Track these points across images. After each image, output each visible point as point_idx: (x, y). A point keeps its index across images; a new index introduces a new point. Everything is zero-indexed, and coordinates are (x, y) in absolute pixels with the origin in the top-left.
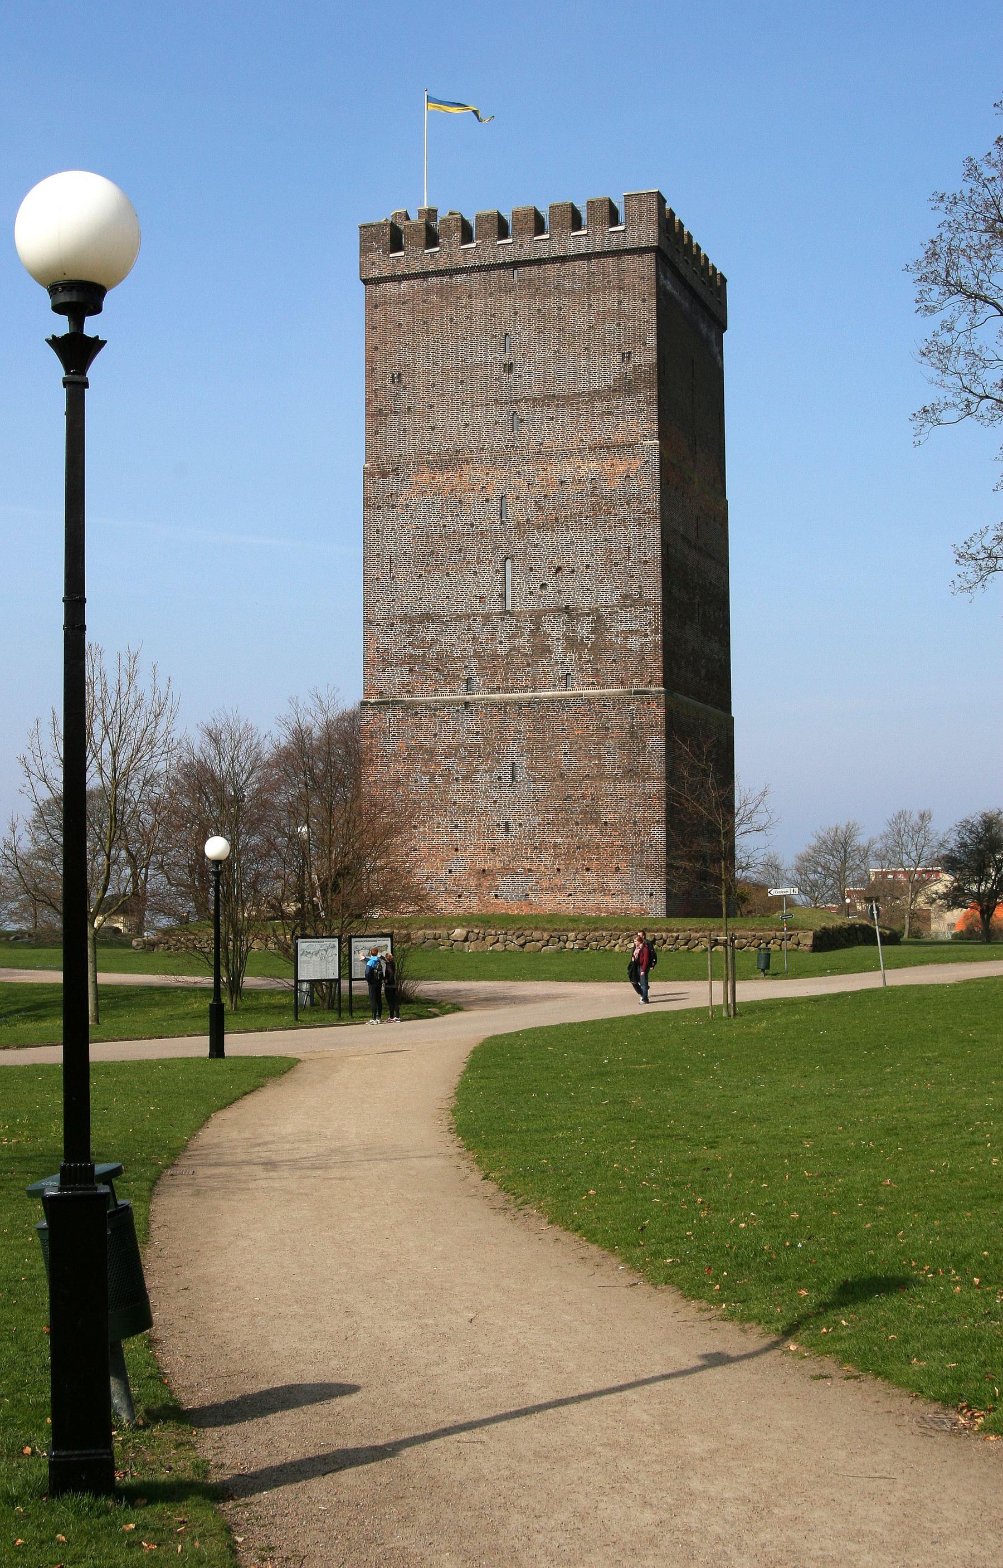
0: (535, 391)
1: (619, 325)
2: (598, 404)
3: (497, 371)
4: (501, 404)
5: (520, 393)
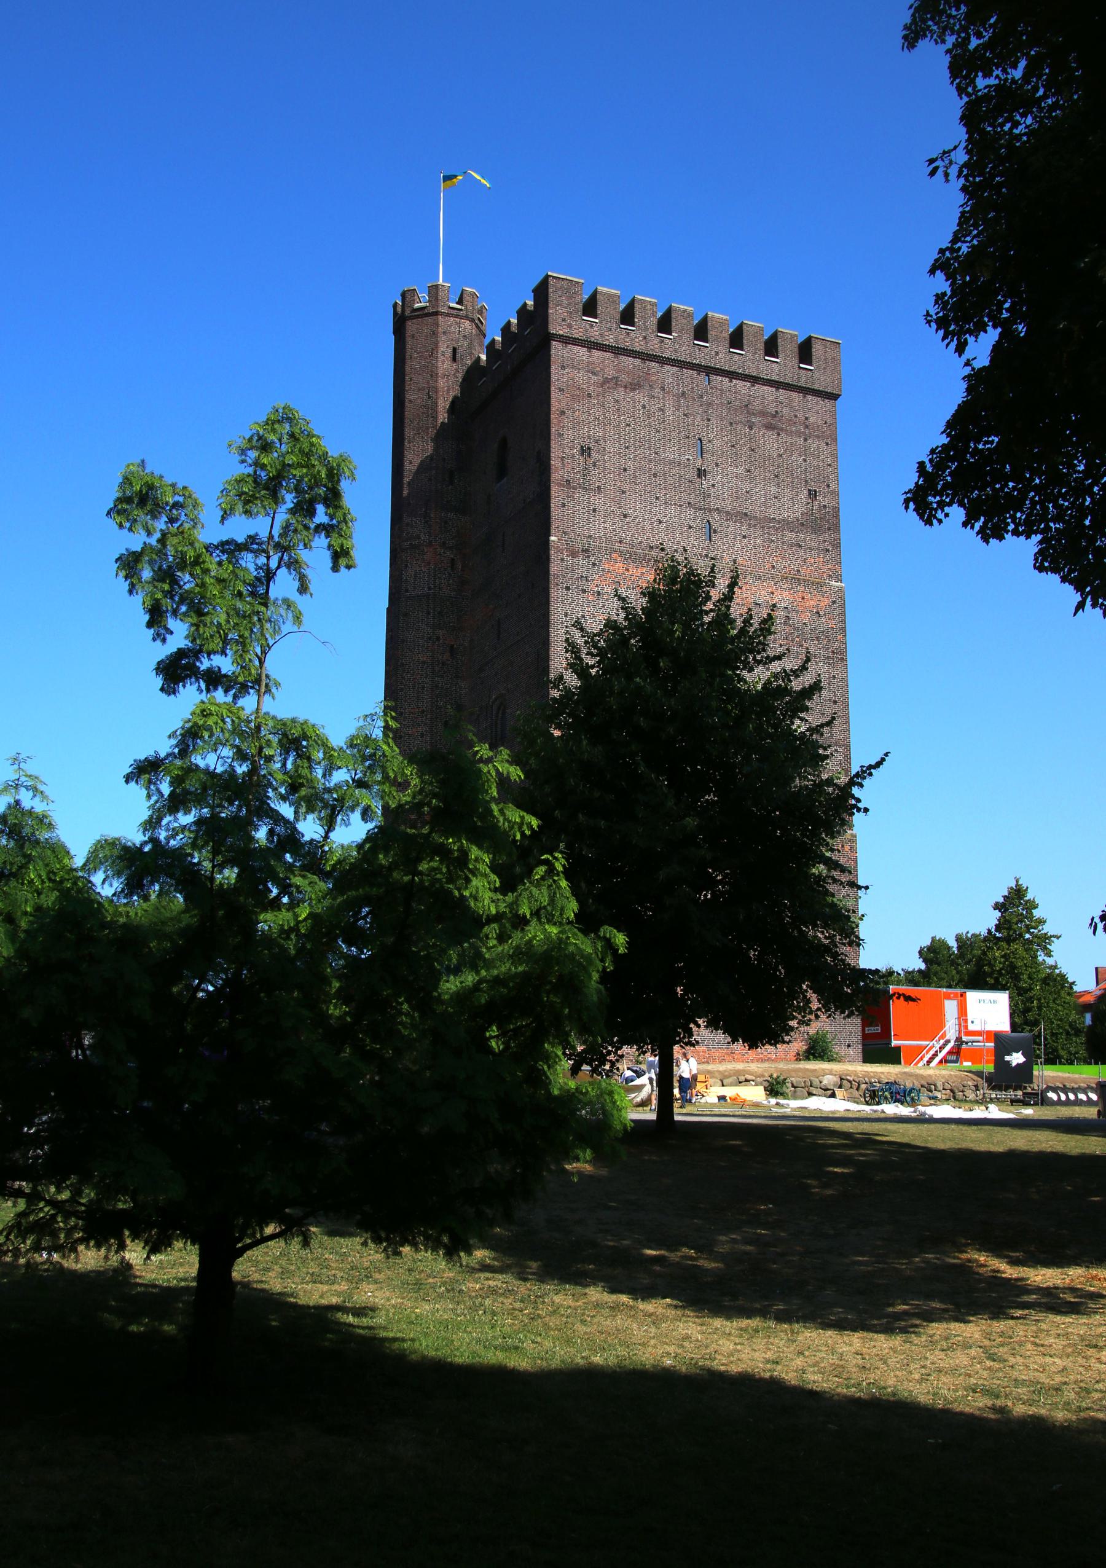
0: (728, 505)
1: (805, 460)
2: (786, 533)
3: (691, 474)
4: (695, 508)
5: (714, 503)
